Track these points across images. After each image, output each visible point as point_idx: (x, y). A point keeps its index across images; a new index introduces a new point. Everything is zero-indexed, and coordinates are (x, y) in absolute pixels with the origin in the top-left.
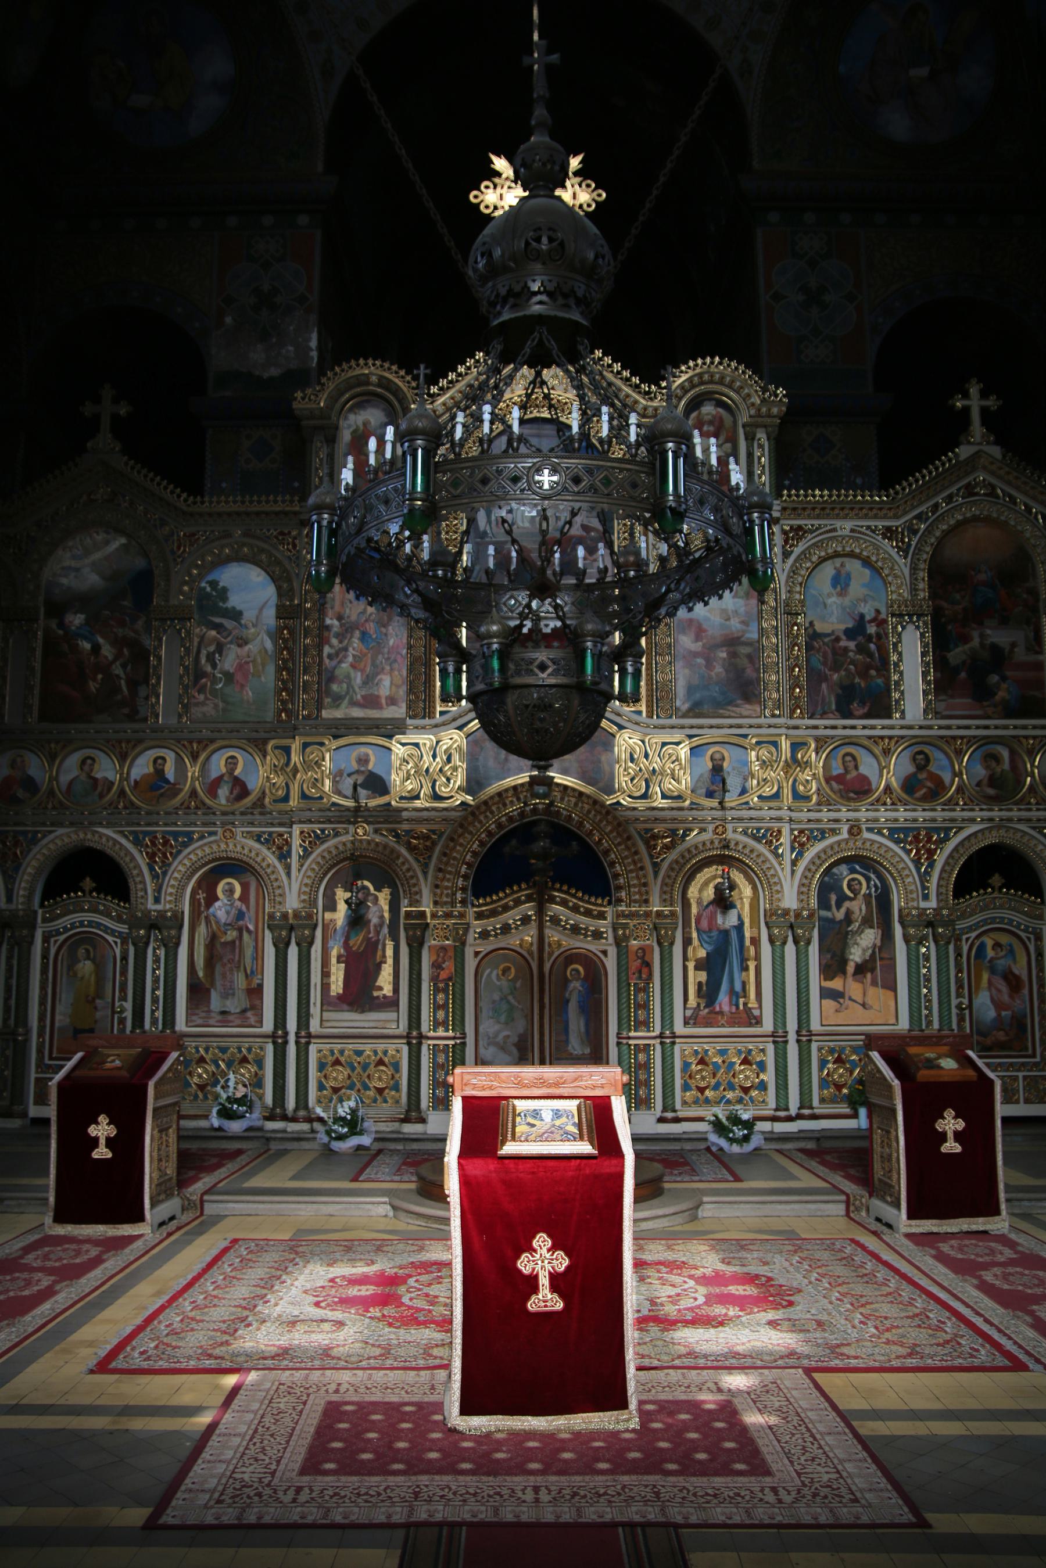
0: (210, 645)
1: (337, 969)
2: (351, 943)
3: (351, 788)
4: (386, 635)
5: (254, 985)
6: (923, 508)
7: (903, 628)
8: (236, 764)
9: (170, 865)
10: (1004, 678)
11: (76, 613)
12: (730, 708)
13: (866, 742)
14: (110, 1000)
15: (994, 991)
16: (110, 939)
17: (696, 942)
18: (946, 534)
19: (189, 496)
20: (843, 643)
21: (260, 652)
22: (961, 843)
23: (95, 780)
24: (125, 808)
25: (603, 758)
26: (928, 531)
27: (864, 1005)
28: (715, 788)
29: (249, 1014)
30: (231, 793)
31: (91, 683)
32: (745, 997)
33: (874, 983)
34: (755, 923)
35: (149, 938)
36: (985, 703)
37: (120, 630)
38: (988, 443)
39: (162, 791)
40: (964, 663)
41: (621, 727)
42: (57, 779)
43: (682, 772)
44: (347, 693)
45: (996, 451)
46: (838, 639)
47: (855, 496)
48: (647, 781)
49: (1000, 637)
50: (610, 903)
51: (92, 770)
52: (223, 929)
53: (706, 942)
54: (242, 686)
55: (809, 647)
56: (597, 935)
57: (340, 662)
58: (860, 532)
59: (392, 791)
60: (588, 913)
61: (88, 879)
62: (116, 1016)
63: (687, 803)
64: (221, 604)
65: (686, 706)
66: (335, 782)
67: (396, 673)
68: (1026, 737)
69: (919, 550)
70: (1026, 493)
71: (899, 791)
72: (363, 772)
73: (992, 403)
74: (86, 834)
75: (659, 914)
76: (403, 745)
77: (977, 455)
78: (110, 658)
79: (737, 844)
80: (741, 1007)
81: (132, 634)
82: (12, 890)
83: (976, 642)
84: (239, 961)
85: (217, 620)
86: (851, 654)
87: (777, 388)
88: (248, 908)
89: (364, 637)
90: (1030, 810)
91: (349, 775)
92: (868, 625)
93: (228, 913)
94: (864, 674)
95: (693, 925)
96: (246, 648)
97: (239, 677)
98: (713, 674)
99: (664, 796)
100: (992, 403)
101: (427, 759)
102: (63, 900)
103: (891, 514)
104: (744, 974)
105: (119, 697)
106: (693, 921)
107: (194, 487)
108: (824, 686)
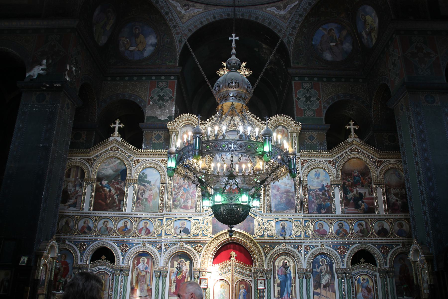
0: (141, 190)
1: (173, 285)
2: (178, 277)
3: (179, 232)
4: (190, 189)
5: (149, 289)
6: (339, 155)
7: (335, 188)
8: (147, 224)
9: (127, 252)
10: (363, 202)
11: (105, 181)
12: (287, 210)
13: (325, 220)
14: (108, 292)
15: (363, 293)
16: (109, 273)
17: (277, 278)
18: (346, 162)
19: (138, 149)
20: (318, 192)
21: (155, 193)
22: (353, 249)
23: (108, 227)
24: (115, 236)
25: (251, 225)
26: (341, 161)
27: (326, 297)
28: (282, 233)
29: (147, 297)
30: (145, 232)
31: (108, 200)
32: (291, 294)
33: (329, 290)
34: (294, 273)
35: (120, 274)
36: (358, 209)
37: (117, 186)
38: (356, 138)
39: (126, 231)
40: (352, 198)
41: (256, 216)
42: (97, 227)
43: (273, 229)
44: (179, 205)
45: (358, 140)
46: (317, 191)
47: (321, 152)
48: (263, 231)
49: (362, 190)
50: (252, 266)
51: (107, 225)
53: (280, 278)
54: (150, 202)
55: (309, 193)
56: (249, 276)
57: (177, 196)
58: (322, 162)
59: (191, 233)
60: (246, 269)
61: (104, 256)
62: (109, 296)
63: (275, 237)
64: (145, 179)
65: (275, 210)
66: (175, 230)
67: (193, 199)
68: (370, 219)
69: (338, 166)
70: (367, 151)
71: (335, 234)
72: (183, 227)
73: (356, 127)
74: (104, 243)
75: (267, 270)
76: (194, 220)
77: (353, 141)
78: (114, 193)
79: (289, 249)
80: (290, 298)
81: (120, 187)
82: (82, 258)
83: (355, 192)
84: (145, 281)
85: (144, 184)
86: (320, 195)
87: (299, 123)
88: (149, 266)
89: (184, 189)
90: (372, 239)
91: (179, 228)
92: (325, 187)
93: (143, 267)
94: (324, 201)
95: (277, 273)
96: (151, 192)
97: (149, 200)
98: (282, 201)
99: (268, 236)
100: (356, 127)
101: (201, 224)
102: (96, 262)
103: (330, 156)
104: (291, 288)
105: (116, 204)
106: (276, 272)
107: (140, 147)
108: (313, 204)
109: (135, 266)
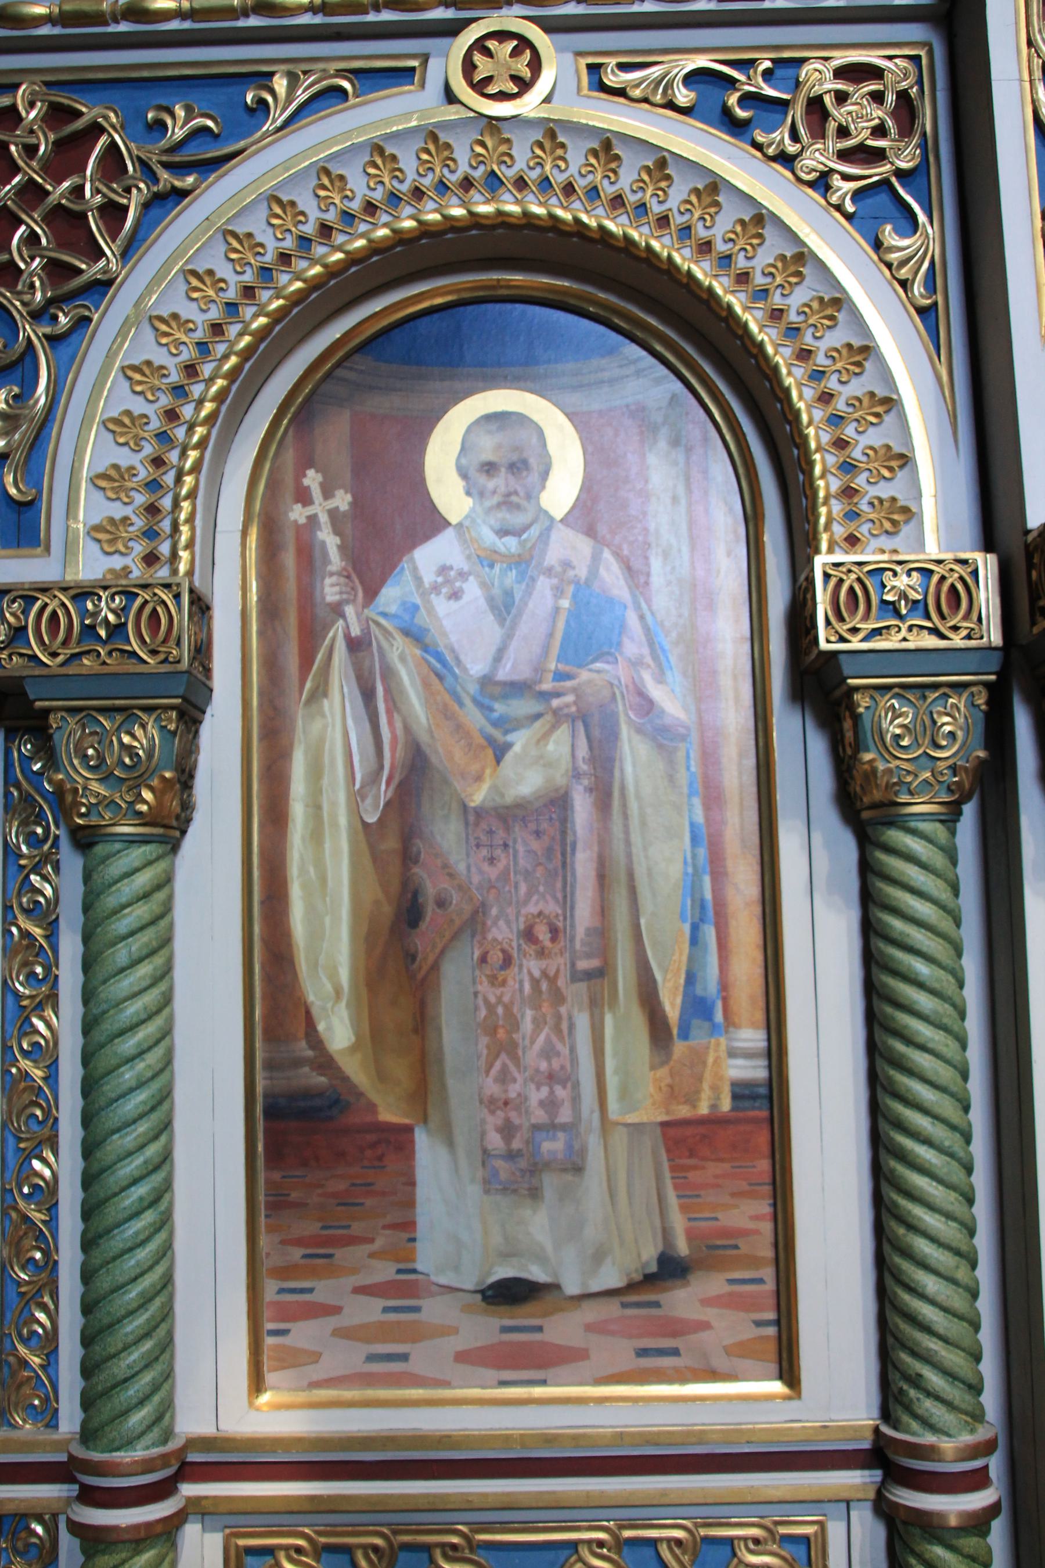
9: (103, 285)
52: (474, 718)
84: (602, 933)
109: (307, 596)
